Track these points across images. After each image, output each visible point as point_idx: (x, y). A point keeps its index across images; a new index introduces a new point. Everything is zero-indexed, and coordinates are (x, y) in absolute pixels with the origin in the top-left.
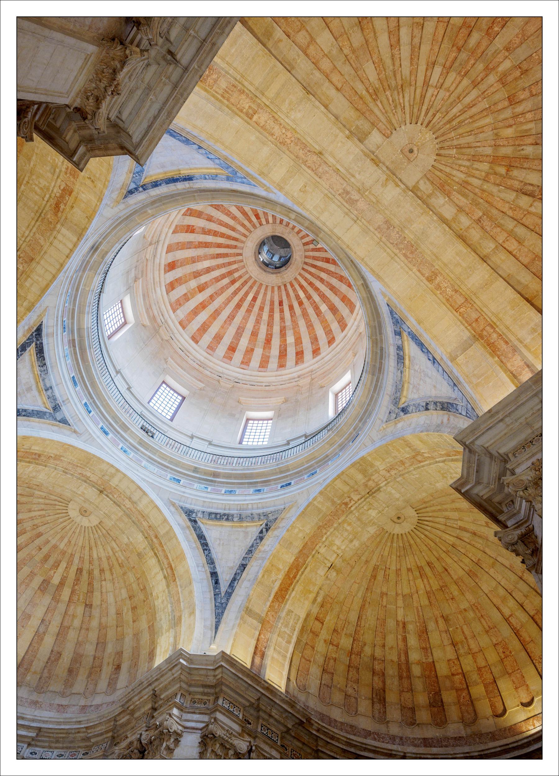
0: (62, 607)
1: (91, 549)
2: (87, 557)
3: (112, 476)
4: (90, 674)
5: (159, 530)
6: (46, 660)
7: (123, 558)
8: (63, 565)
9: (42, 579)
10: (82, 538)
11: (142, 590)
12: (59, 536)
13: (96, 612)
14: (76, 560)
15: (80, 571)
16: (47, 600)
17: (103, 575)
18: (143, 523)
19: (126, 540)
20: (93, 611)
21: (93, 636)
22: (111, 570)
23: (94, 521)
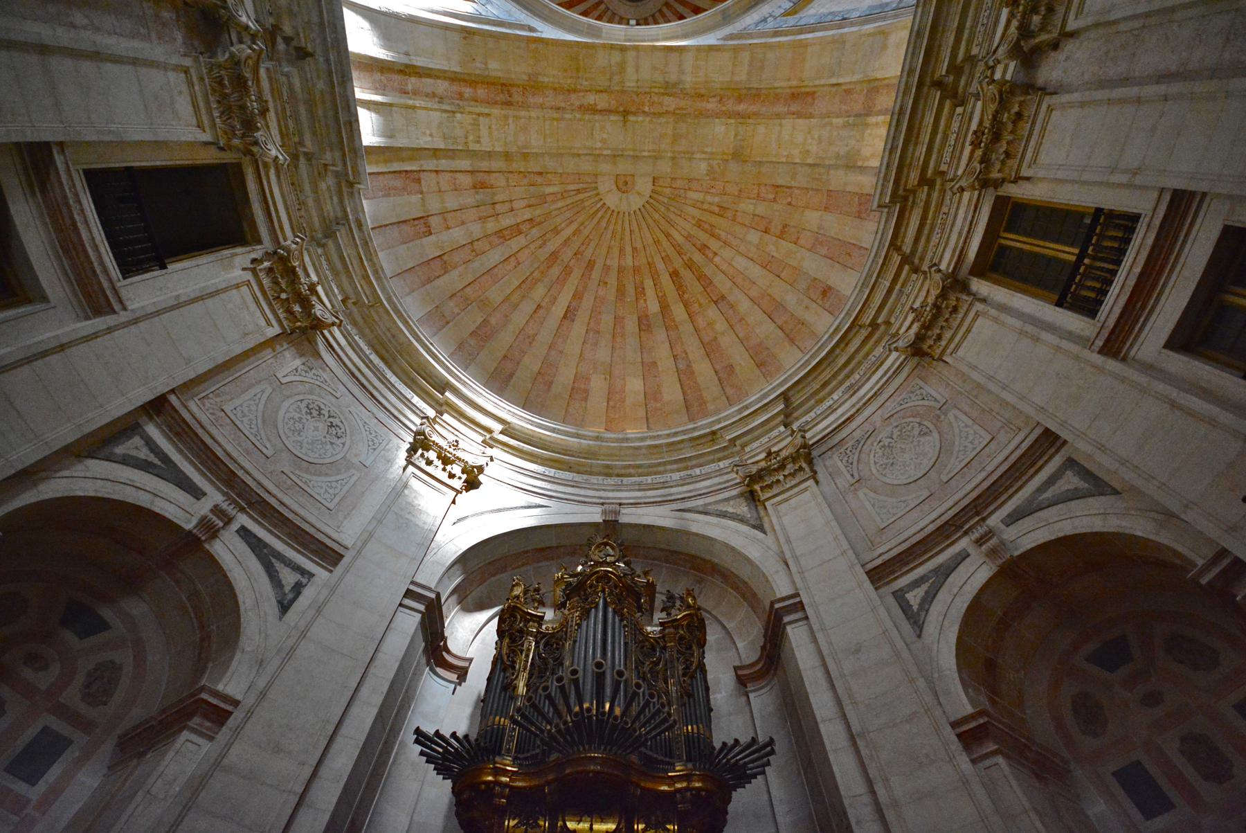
0: (687, 328)
1: (668, 236)
2: (670, 251)
3: (622, 66)
4: (792, 341)
5: (736, 78)
6: (717, 382)
7: (717, 199)
8: (649, 283)
9: (635, 318)
10: (646, 230)
11: (774, 200)
12: (616, 251)
13: (736, 296)
14: (660, 266)
15: (675, 275)
16: (661, 335)
17: (707, 252)
18: (710, 106)
19: (703, 166)
20: (731, 298)
21: (755, 316)
22: (712, 235)
23: (644, 186)
